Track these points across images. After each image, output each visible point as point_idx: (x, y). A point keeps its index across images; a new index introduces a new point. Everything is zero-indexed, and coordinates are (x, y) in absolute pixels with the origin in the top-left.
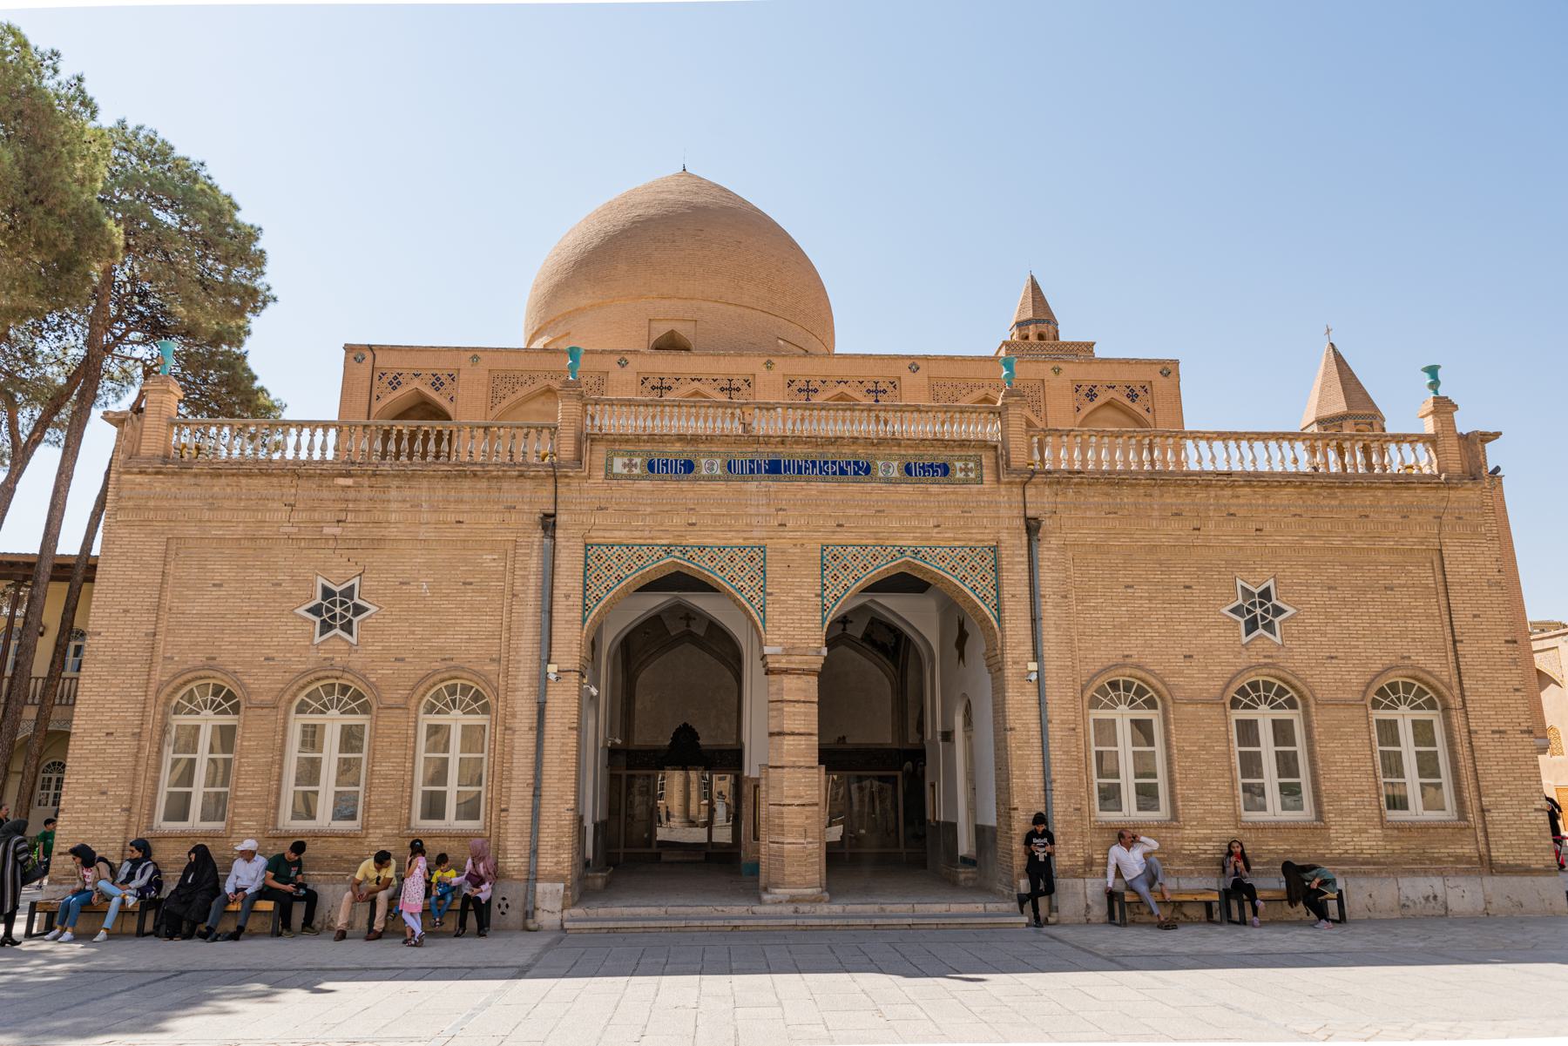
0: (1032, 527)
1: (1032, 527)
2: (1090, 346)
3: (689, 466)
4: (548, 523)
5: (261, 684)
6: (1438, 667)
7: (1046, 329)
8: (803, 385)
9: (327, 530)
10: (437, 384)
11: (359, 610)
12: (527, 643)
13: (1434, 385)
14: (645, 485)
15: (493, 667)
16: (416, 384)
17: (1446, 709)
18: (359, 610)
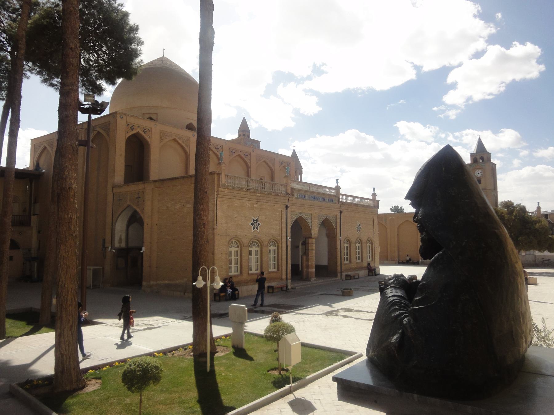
0: (341, 212)
1: (341, 212)
2: (258, 142)
3: (304, 196)
4: (287, 207)
5: (245, 241)
6: (372, 237)
7: (246, 134)
8: (231, 150)
9: (255, 206)
10: (145, 131)
11: (259, 224)
12: (284, 233)
13: (374, 190)
14: (300, 200)
15: (279, 238)
16: (138, 130)
17: (372, 244)
18: (259, 224)
